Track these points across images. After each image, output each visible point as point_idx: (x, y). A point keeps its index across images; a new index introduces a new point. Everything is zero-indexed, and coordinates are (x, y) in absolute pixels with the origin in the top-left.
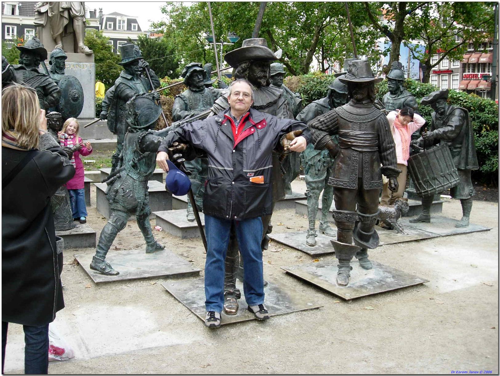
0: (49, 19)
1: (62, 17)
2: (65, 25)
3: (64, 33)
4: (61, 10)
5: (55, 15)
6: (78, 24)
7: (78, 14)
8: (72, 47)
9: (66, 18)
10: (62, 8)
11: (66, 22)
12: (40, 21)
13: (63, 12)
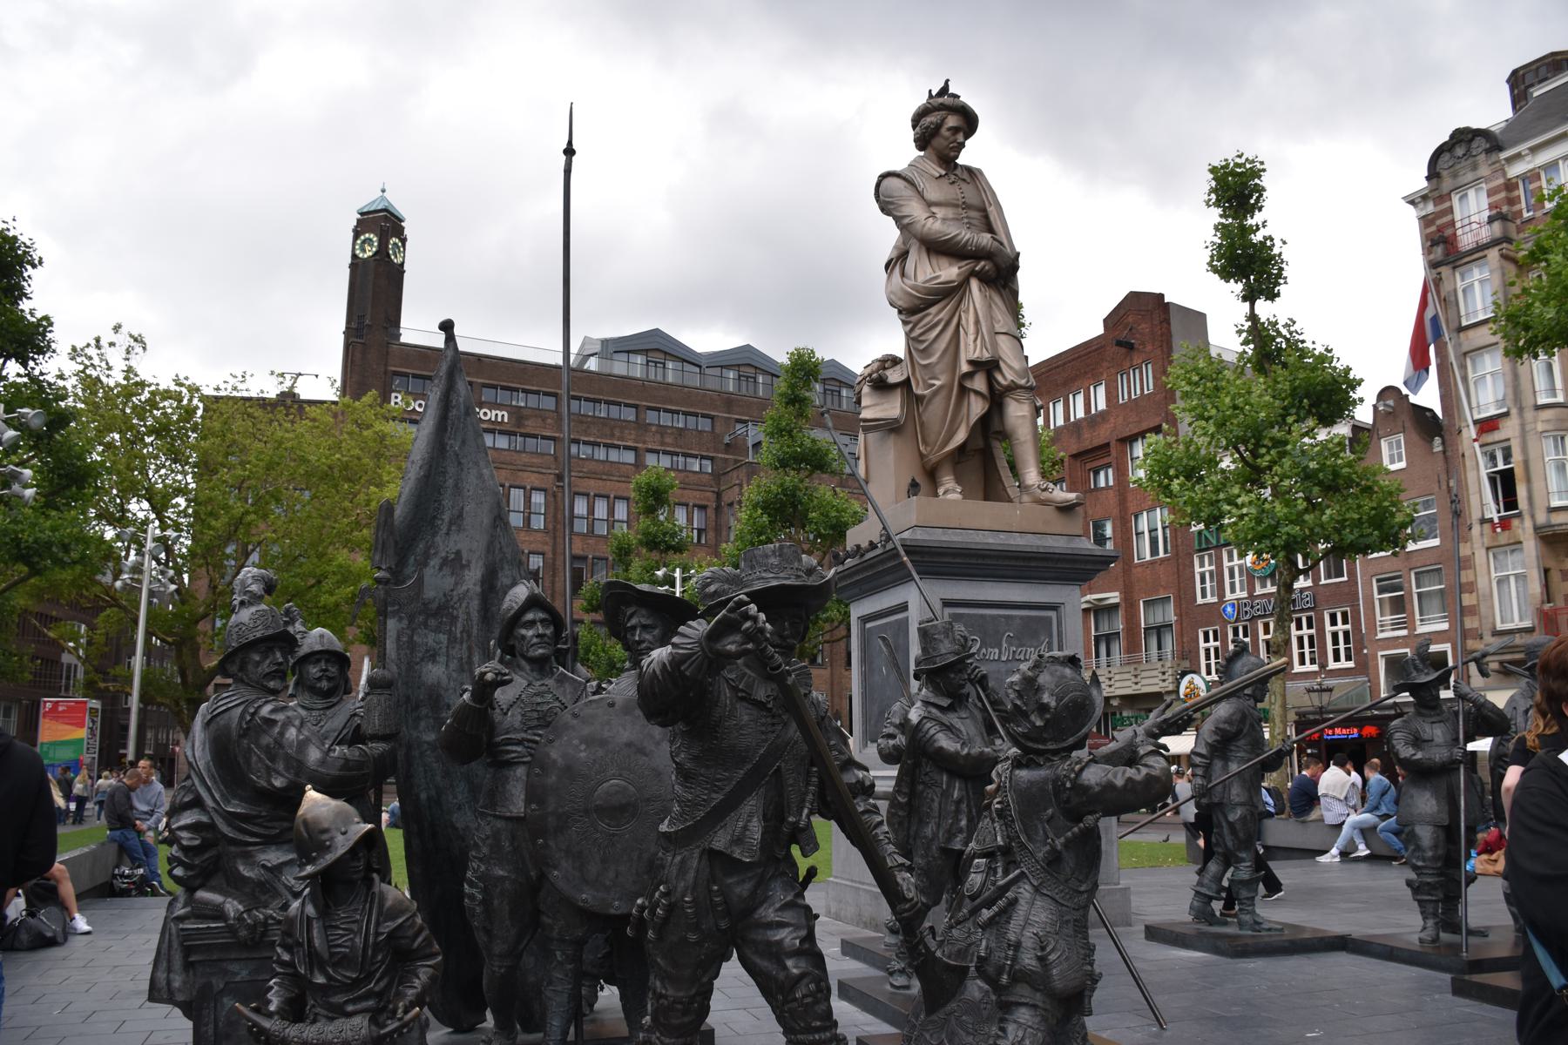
2: (974, 418)
4: (965, 368)
8: (981, 494)
9: (977, 393)
11: (977, 408)
13: (969, 375)
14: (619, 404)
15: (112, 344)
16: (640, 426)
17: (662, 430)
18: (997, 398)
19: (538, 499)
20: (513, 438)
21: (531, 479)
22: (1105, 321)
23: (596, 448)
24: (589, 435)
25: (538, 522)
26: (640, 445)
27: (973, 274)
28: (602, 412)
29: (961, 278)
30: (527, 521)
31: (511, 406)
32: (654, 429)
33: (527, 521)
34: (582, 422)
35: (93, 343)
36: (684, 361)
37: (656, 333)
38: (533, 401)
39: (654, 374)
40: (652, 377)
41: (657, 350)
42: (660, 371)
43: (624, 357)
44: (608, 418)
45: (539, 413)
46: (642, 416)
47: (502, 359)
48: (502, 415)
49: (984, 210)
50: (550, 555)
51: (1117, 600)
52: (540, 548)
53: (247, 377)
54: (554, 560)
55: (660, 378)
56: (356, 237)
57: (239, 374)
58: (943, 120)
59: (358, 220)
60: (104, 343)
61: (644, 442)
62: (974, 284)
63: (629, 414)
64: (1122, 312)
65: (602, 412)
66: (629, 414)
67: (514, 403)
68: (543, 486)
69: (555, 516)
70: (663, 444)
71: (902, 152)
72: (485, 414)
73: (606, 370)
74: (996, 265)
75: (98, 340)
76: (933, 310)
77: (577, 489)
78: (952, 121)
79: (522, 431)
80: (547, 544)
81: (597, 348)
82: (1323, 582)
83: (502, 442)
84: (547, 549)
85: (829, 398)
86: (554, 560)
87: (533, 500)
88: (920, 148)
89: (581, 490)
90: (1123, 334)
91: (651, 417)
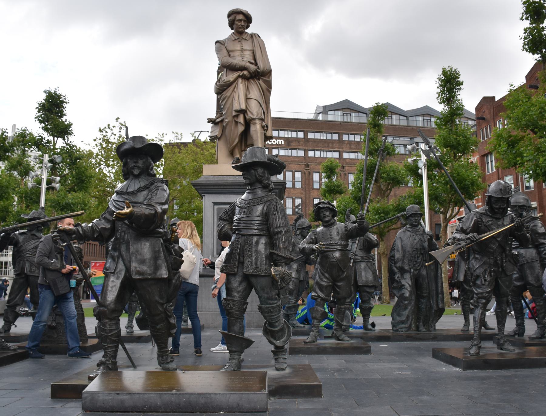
0: (224, 129)
1: (237, 123)
2: (239, 133)
3: (239, 145)
4: (234, 114)
5: (229, 122)
6: (256, 129)
7: (252, 117)
9: (240, 123)
10: (236, 111)
11: (241, 128)
12: (215, 133)
13: (237, 116)
14: (331, 133)
15: (114, 127)
16: (340, 141)
17: (350, 142)
18: (248, 124)
19: (298, 175)
20: (286, 151)
21: (295, 167)
22: (526, 77)
23: (322, 152)
24: (319, 147)
25: (298, 185)
26: (341, 150)
27: (239, 76)
28: (323, 136)
29: (232, 80)
30: (294, 185)
31: (285, 137)
32: (346, 142)
33: (294, 185)
34: (315, 142)
35: (107, 127)
36: (359, 112)
37: (347, 101)
38: (294, 135)
39: (347, 119)
40: (345, 120)
41: (347, 108)
42: (349, 117)
43: (332, 112)
44: (326, 139)
45: (297, 140)
46: (341, 137)
47: (280, 118)
48: (282, 142)
49: (253, 50)
50: (304, 199)
51: (536, 206)
52: (300, 195)
53: (164, 135)
54: (306, 200)
55: (349, 120)
56: (218, 74)
57: (161, 134)
58: (235, 17)
59: (219, 67)
60: (111, 127)
61: (343, 148)
62: (240, 80)
63: (336, 137)
64: (533, 72)
65: (323, 136)
66: (336, 137)
67: (286, 136)
68: (300, 170)
69: (305, 181)
70: (351, 148)
71: (226, 32)
72: (274, 142)
73: (325, 119)
74: (249, 72)
75: (109, 125)
76: (224, 93)
77: (314, 170)
78: (241, 17)
79: (290, 147)
80: (302, 194)
81: (321, 110)
82: (525, 191)
83: (282, 153)
84: (303, 196)
85: (426, 123)
86: (306, 200)
87: (296, 176)
88: (232, 29)
89: (316, 171)
90: (533, 83)
91: (345, 137)
